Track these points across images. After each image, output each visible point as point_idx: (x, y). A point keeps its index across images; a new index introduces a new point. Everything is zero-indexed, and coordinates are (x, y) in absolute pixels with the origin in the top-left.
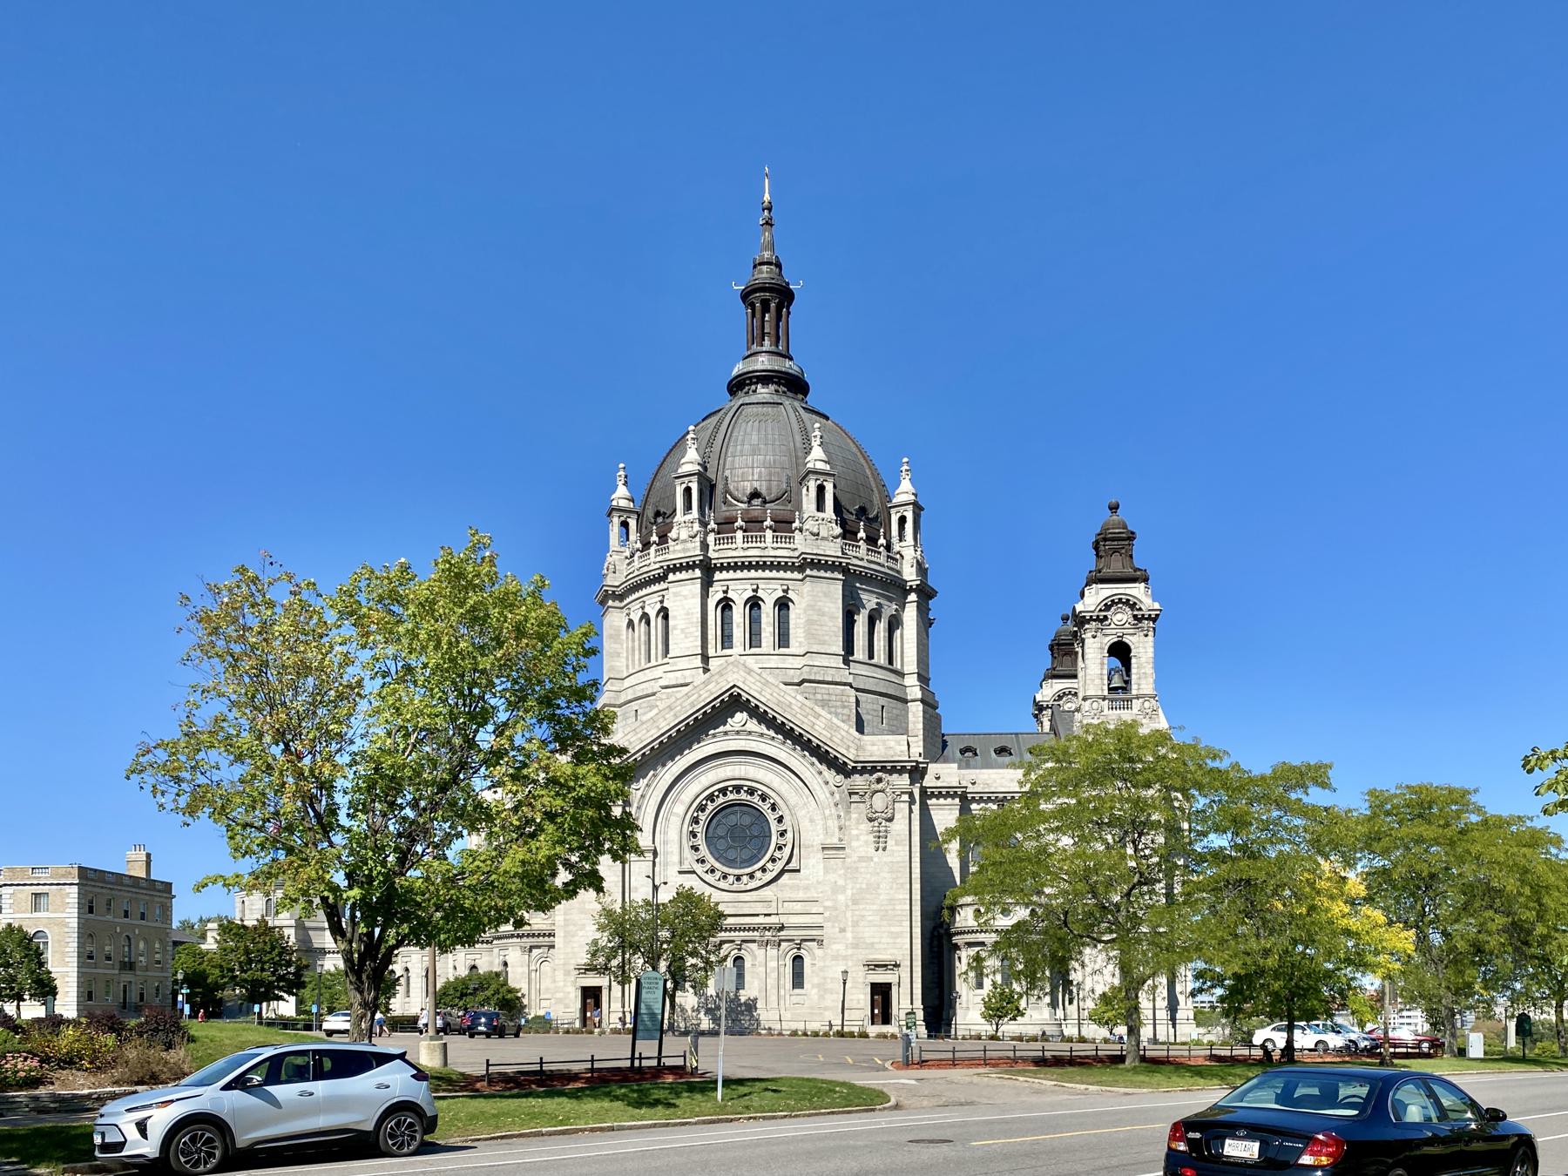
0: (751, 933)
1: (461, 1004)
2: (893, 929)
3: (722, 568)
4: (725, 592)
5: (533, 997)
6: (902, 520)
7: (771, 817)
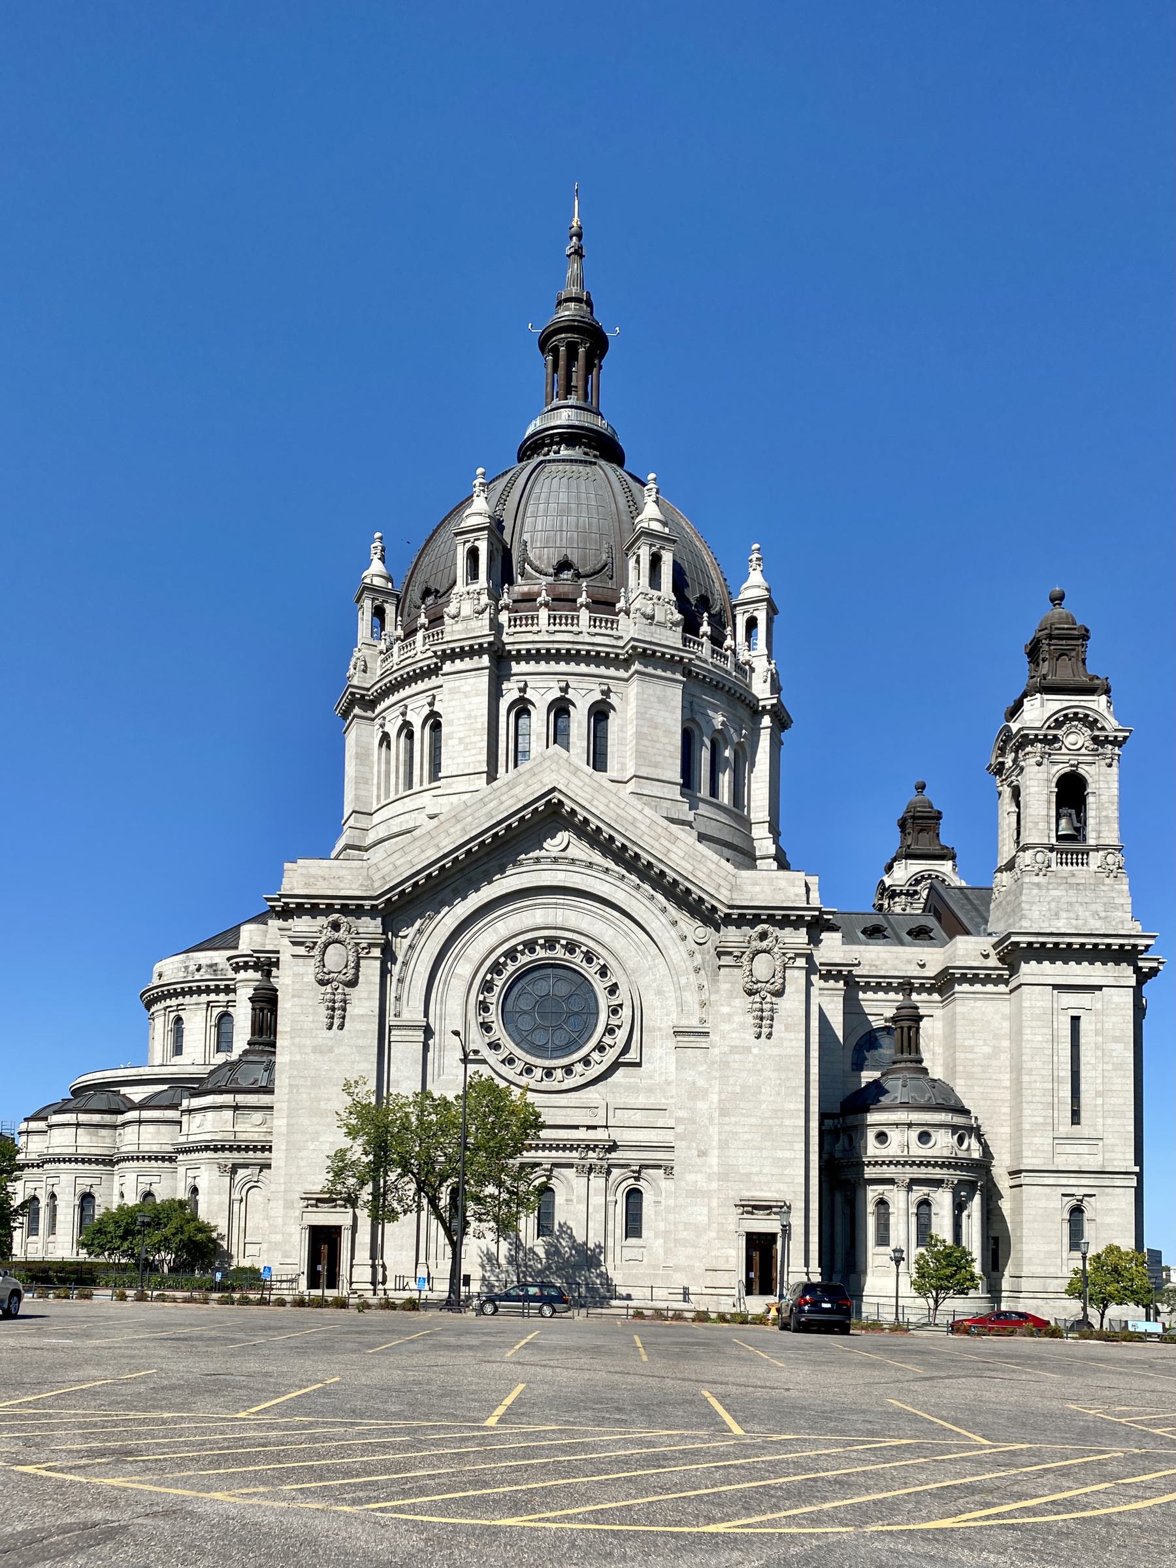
0: (567, 1154)
1: (125, 1246)
3: (519, 657)
4: (523, 690)
5: (235, 1240)
6: (752, 624)
7: (600, 986)
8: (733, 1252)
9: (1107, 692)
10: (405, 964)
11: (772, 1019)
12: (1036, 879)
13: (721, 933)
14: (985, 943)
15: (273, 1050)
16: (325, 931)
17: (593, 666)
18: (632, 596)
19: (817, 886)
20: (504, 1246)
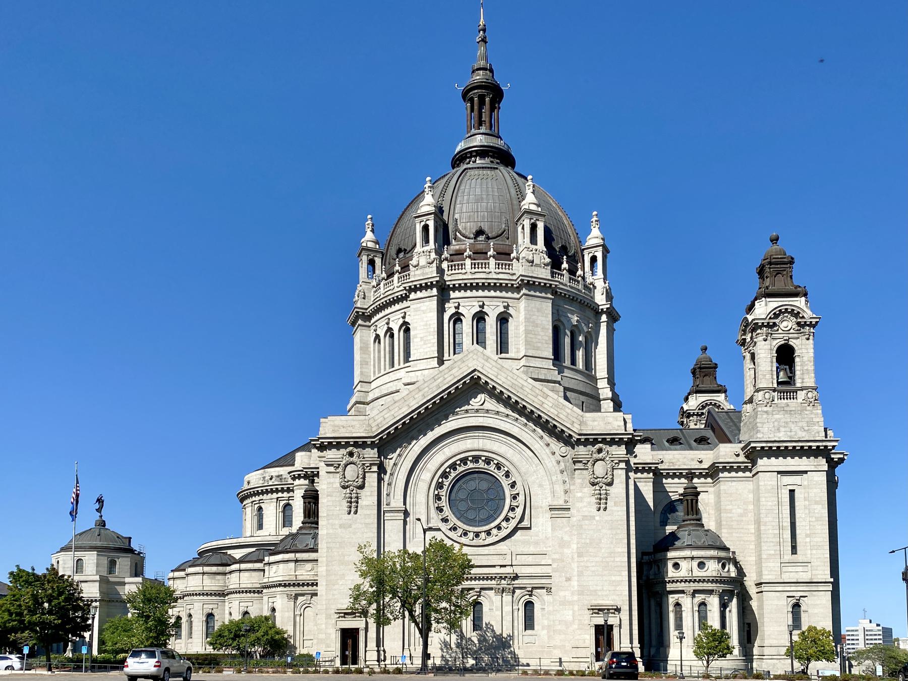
0: (489, 582)
2: (613, 578)
3: (454, 288)
4: (457, 308)
5: (298, 639)
7: (505, 483)
8: (588, 637)
9: (805, 295)
10: (391, 474)
11: (607, 499)
12: (765, 409)
13: (575, 450)
14: (737, 447)
15: (316, 526)
16: (345, 457)
17: (498, 292)
18: (521, 249)
19: (631, 421)
20: (454, 637)
